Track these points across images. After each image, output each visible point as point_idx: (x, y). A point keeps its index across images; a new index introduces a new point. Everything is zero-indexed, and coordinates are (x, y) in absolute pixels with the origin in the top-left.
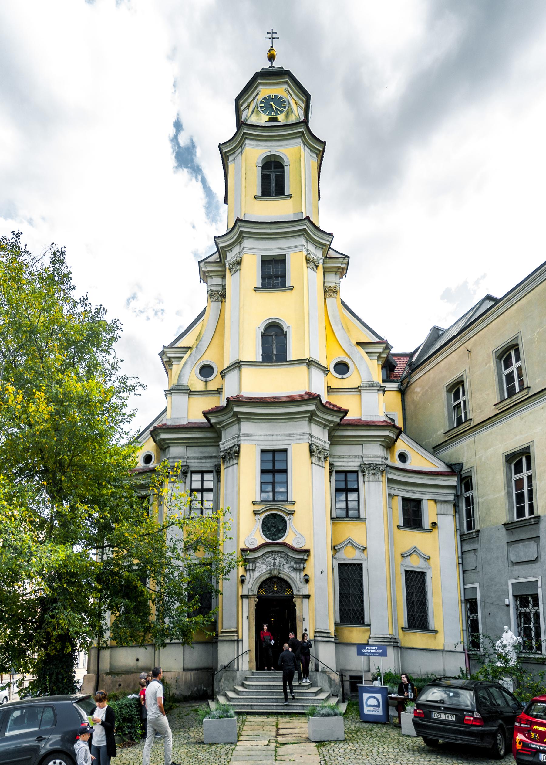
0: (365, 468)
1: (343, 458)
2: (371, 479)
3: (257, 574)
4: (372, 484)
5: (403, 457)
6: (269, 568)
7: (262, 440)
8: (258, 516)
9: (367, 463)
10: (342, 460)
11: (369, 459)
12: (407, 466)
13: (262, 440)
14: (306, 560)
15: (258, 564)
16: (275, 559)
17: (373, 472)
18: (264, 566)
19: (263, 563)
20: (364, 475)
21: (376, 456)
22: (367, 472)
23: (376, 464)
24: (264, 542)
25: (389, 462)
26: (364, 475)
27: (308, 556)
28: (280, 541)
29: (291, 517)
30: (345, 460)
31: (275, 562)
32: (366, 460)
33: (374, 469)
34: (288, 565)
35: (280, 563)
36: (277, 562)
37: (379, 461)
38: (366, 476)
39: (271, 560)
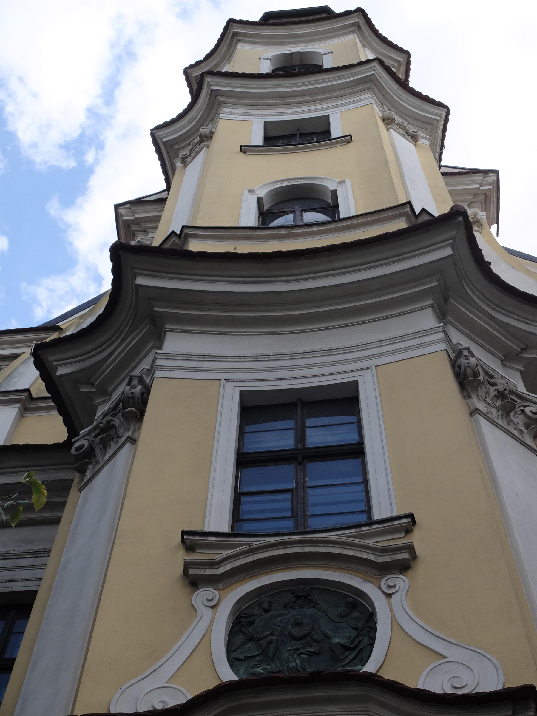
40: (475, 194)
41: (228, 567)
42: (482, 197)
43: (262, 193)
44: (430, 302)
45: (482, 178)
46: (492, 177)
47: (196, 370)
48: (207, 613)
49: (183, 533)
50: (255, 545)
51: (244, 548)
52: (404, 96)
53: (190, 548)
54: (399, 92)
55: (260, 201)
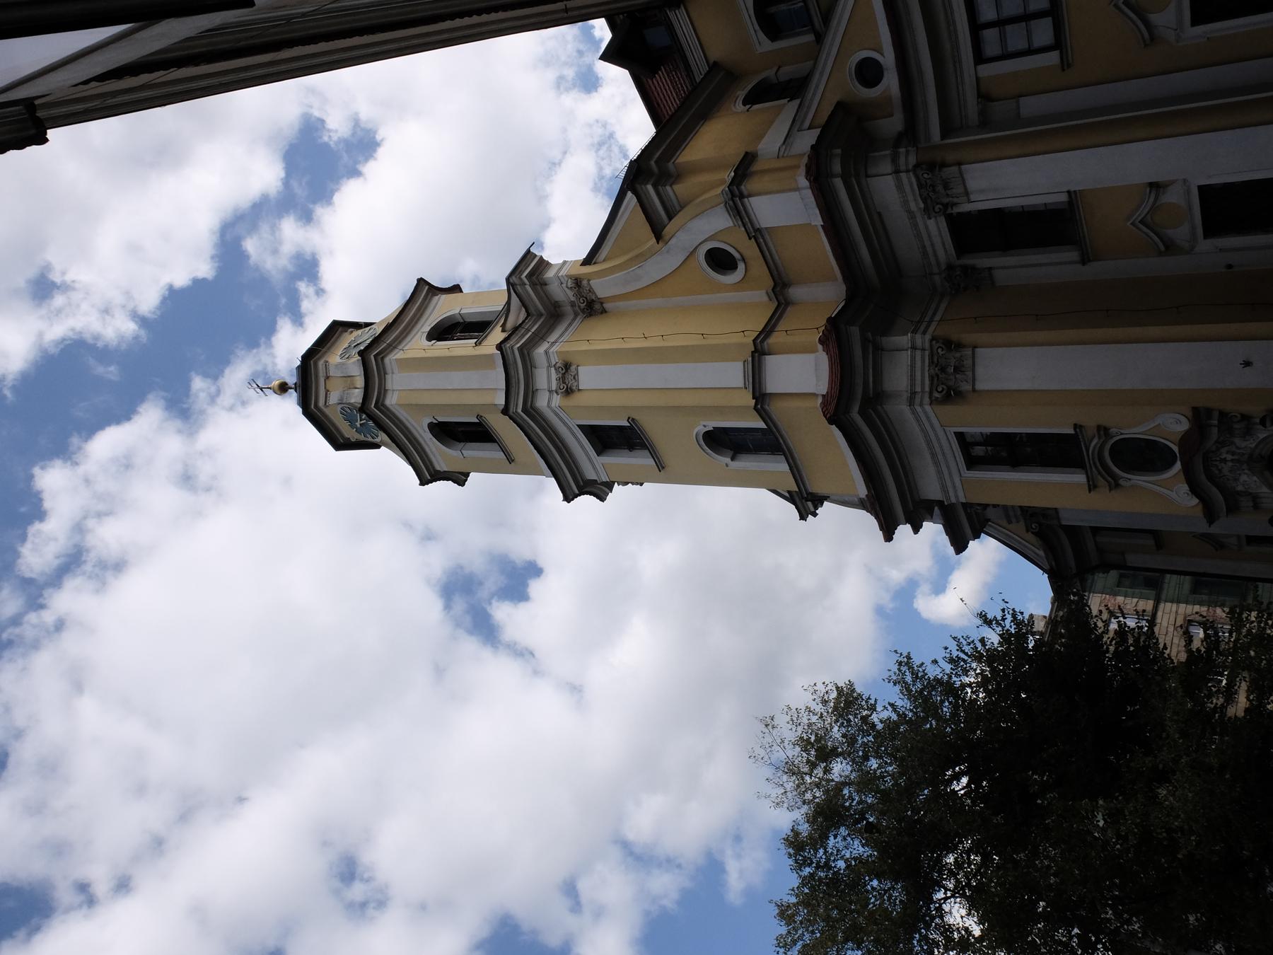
0: (937, 210)
1: (924, 247)
2: (960, 190)
3: (1265, 489)
4: (972, 184)
5: (869, 72)
6: (1246, 471)
7: (948, 467)
8: (1121, 482)
9: (922, 205)
10: (929, 250)
11: (910, 198)
12: (888, 58)
13: (948, 467)
14: (1223, 414)
15: (1240, 488)
16: (1225, 461)
17: (940, 188)
18: (1244, 478)
19: (1236, 480)
20: (956, 204)
21: (900, 187)
22: (946, 200)
23: (920, 186)
24: (1182, 477)
25: (893, 124)
26: (956, 204)
27: (1209, 411)
28: (1176, 449)
29: (1113, 431)
30: (927, 243)
31: (1232, 460)
32: (916, 205)
33: (933, 186)
34: (1237, 441)
35: (1233, 454)
36: (1229, 457)
37: (908, 180)
38: (955, 200)
39: (1226, 469)
40: (533, 285)
41: (1109, 479)
42: (534, 278)
43: (728, 460)
44: (879, 407)
45: (518, 287)
46: (514, 279)
47: (954, 487)
48: (1132, 482)
49: (1090, 491)
50: (1096, 472)
51: (1099, 477)
52: (514, 380)
53: (1095, 487)
54: (514, 385)
55: (732, 459)
